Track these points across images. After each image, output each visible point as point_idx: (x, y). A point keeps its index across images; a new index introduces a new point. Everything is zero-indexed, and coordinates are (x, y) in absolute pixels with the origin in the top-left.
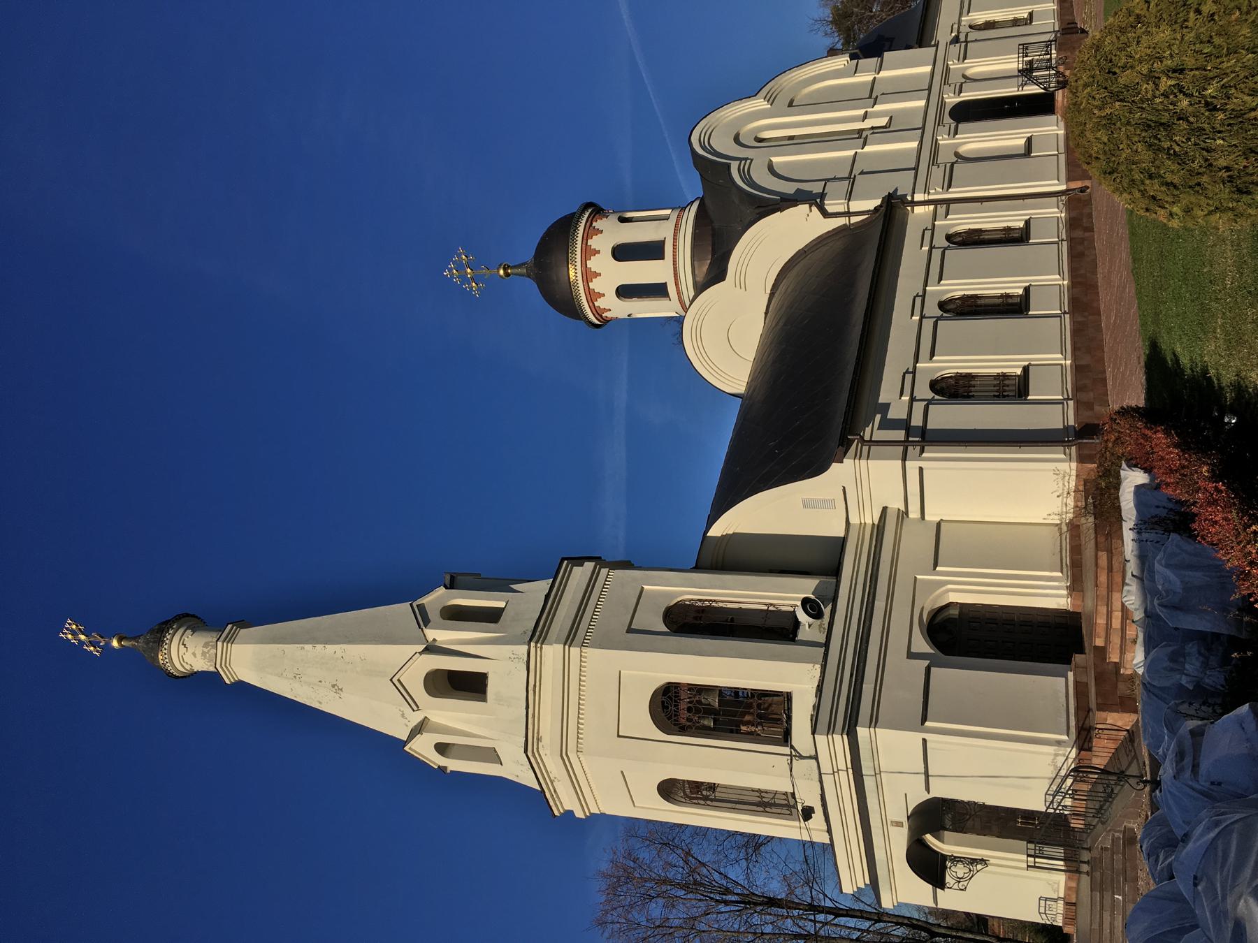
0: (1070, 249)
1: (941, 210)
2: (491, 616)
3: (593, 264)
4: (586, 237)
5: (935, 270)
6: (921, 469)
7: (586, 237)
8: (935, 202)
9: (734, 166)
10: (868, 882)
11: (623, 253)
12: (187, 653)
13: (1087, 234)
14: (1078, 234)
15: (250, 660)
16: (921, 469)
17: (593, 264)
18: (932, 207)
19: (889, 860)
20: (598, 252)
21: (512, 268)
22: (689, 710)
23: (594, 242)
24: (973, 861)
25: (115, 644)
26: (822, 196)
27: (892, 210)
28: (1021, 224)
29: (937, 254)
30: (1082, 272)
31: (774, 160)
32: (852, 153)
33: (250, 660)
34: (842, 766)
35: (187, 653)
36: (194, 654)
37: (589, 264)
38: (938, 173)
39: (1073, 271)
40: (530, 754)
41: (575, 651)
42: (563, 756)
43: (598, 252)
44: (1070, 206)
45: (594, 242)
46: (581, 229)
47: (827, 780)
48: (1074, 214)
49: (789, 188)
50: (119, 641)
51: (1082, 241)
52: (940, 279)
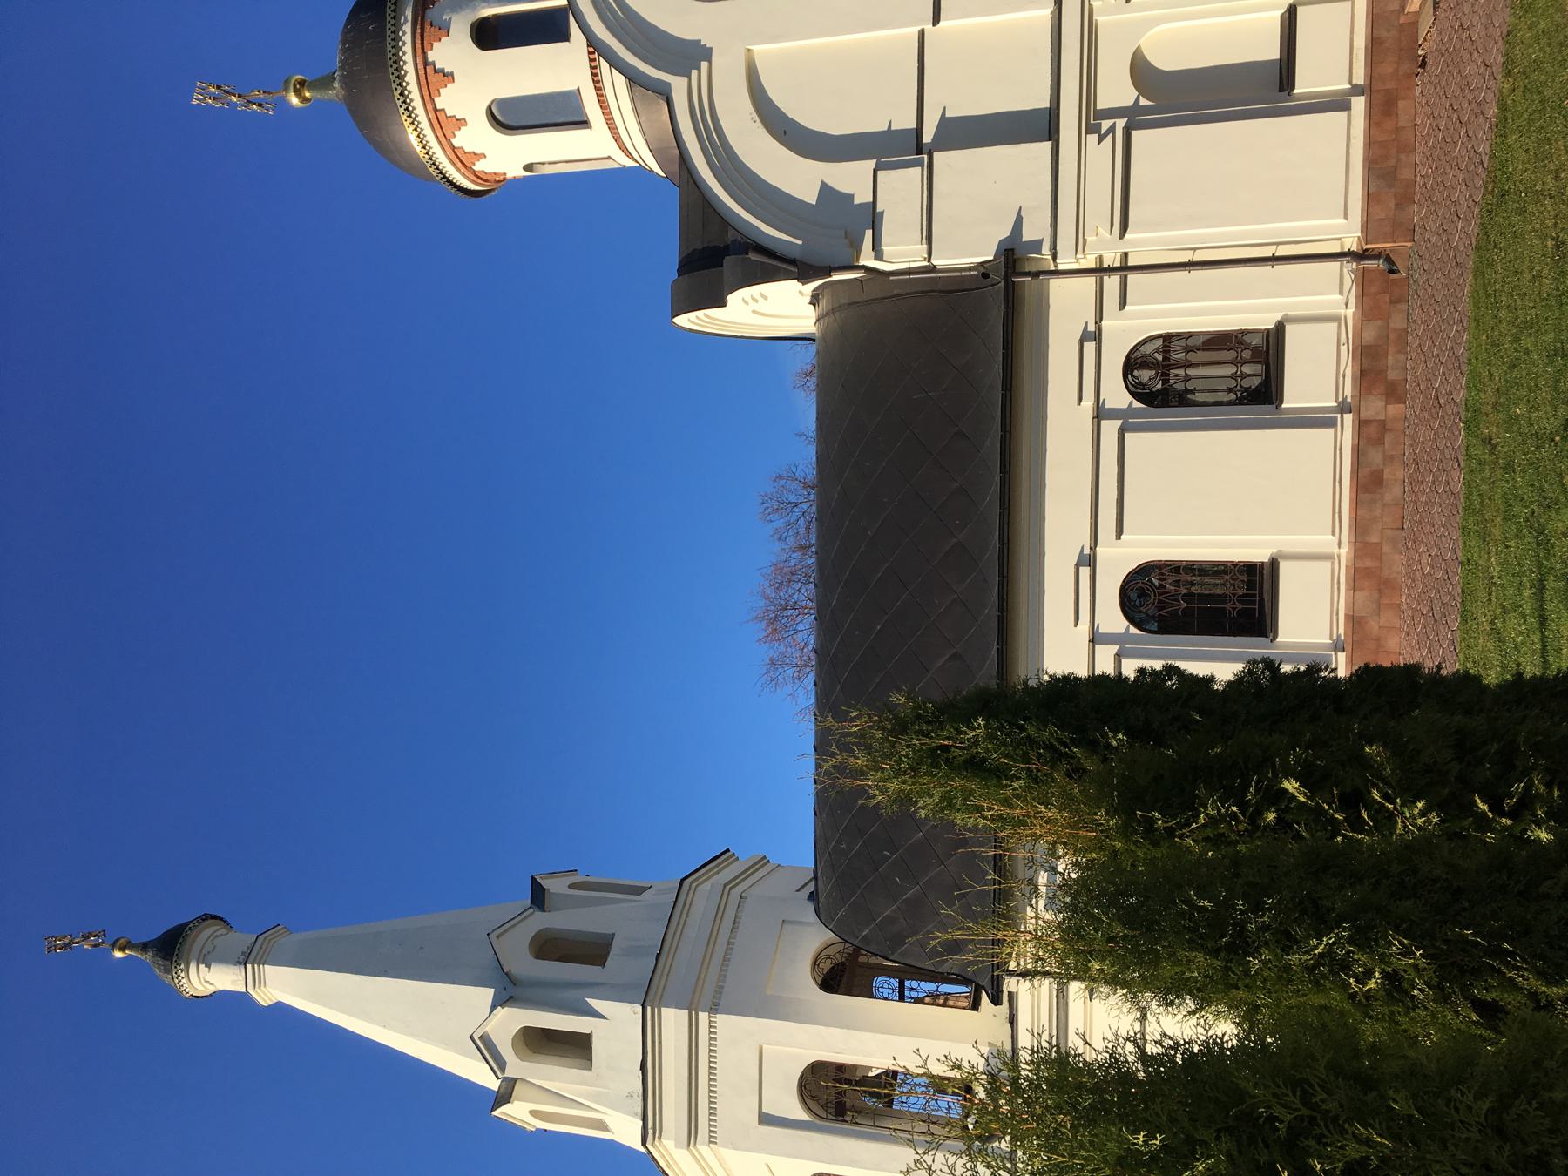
0: (1358, 452)
1: (1112, 283)
2: (576, 1047)
3: (461, 139)
4: (428, 95)
5: (1110, 507)
7: (428, 95)
8: (1100, 270)
9: (678, 85)
11: (510, 117)
13: (1395, 410)
14: (1375, 407)
17: (461, 139)
18: (1091, 281)
20: (461, 122)
21: (313, 86)
23: (447, 100)
25: (118, 954)
26: (872, 217)
27: (1012, 274)
28: (1267, 322)
29: (1110, 428)
30: (1374, 539)
31: (755, 48)
32: (915, 30)
37: (456, 142)
38: (1100, 155)
39: (1359, 528)
41: (703, 1149)
43: (461, 122)
44: (1363, 279)
45: (447, 100)
46: (411, 78)
48: (1370, 335)
49: (800, 178)
50: (123, 949)
51: (1383, 426)
52: (1120, 532)
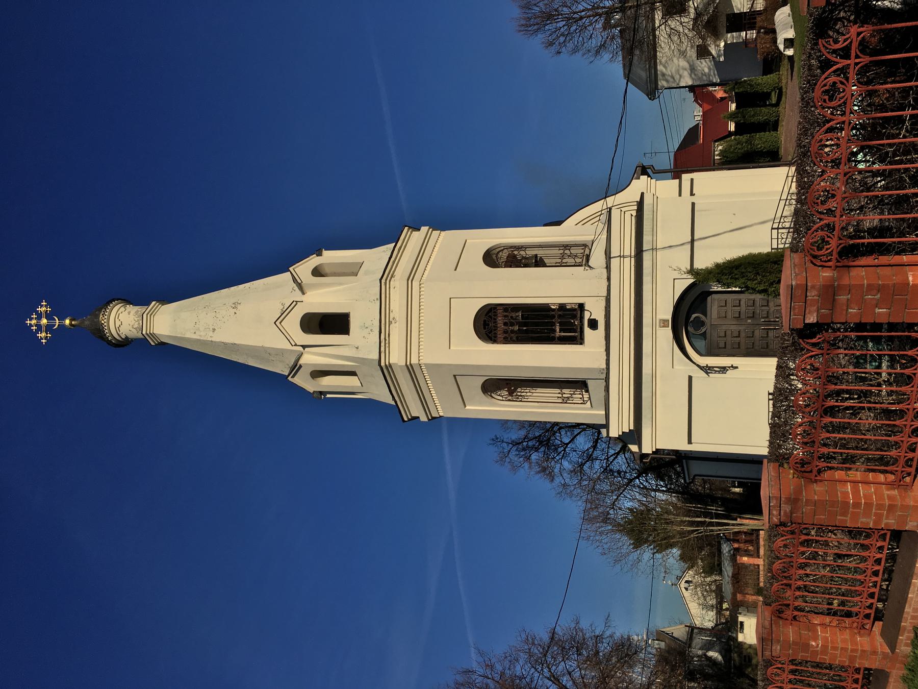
6: (692, 180)
10: (632, 428)
12: (122, 320)
15: (171, 322)
16: (692, 180)
19: (654, 376)
22: (505, 324)
24: (723, 370)
33: (171, 322)
34: (627, 253)
35: (122, 320)
36: (129, 313)
40: (383, 281)
42: (410, 278)
47: (615, 263)
50: (71, 320)
